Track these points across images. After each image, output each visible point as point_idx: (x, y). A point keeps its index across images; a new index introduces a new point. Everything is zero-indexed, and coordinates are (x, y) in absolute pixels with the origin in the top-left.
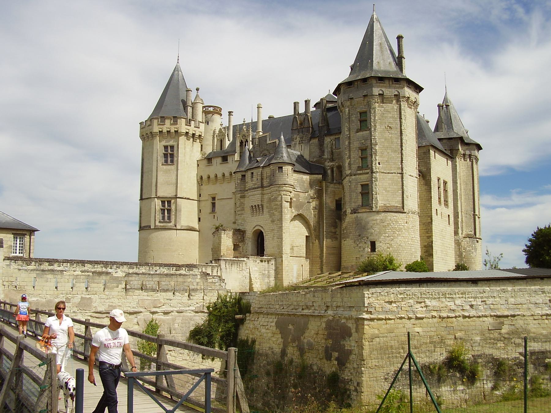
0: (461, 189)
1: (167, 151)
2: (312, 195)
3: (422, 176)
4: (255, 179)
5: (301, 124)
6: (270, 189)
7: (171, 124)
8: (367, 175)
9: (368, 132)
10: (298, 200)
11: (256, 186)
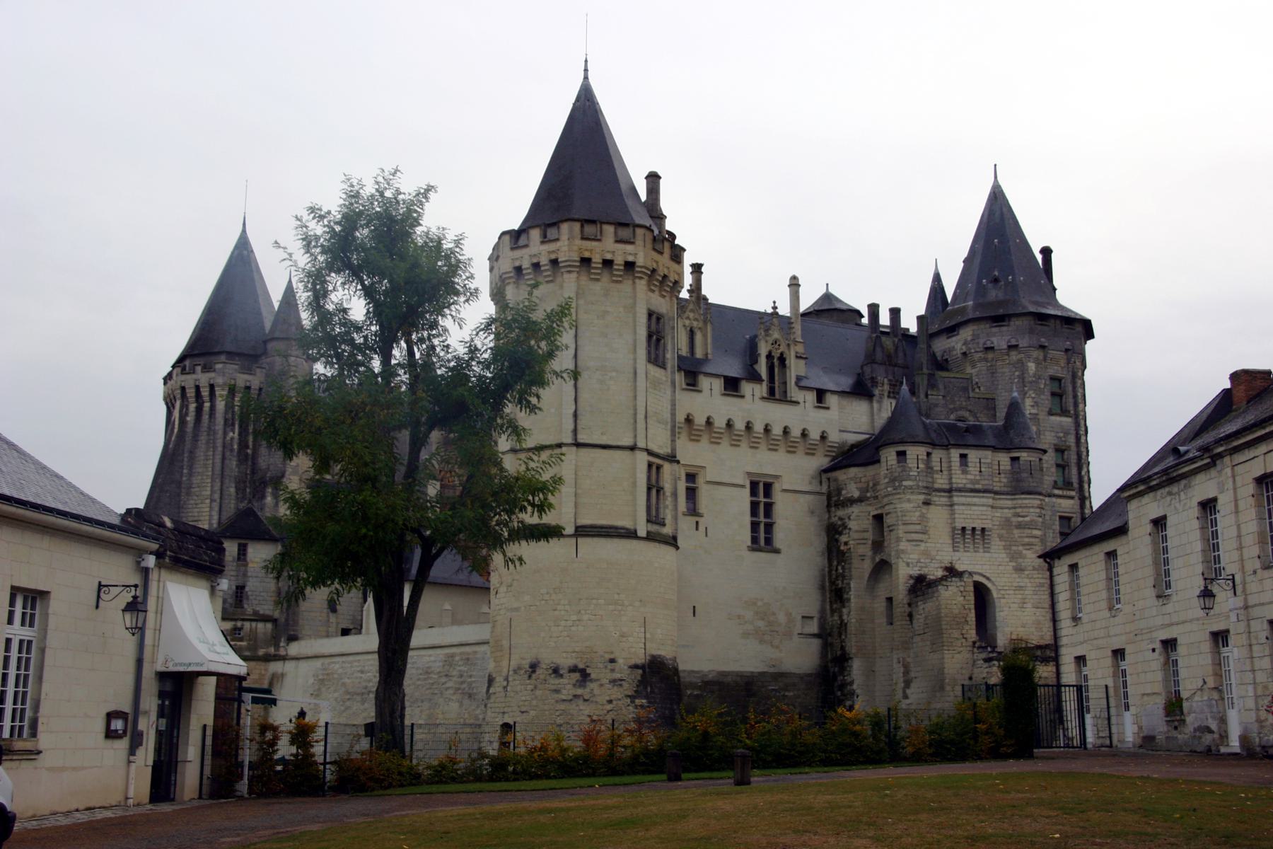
4: (973, 468)
6: (1012, 499)
8: (1071, 502)
9: (1069, 420)
11: (977, 487)
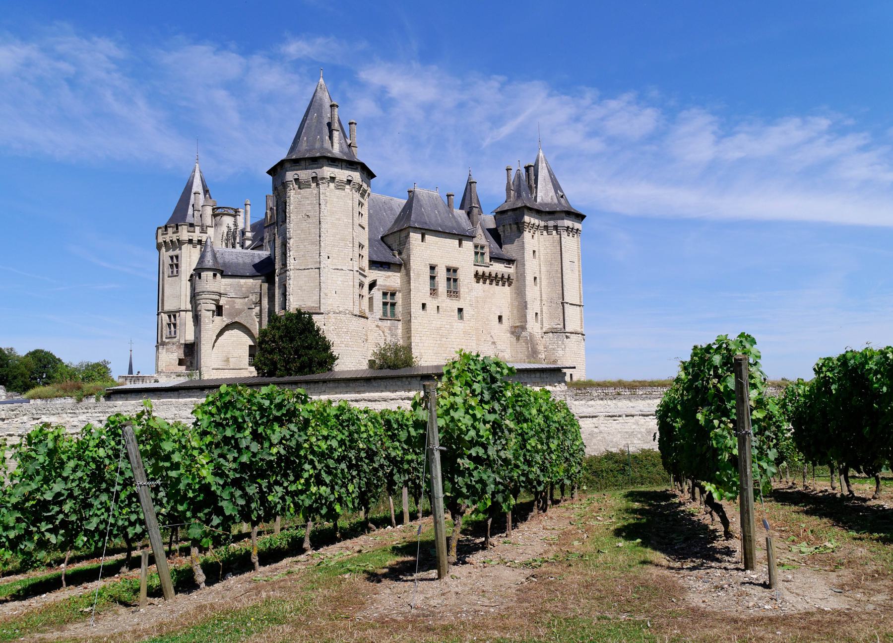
0: (540, 271)
1: (172, 261)
2: (254, 300)
3: (405, 267)
5: (270, 219)
7: (173, 233)
10: (232, 307)
